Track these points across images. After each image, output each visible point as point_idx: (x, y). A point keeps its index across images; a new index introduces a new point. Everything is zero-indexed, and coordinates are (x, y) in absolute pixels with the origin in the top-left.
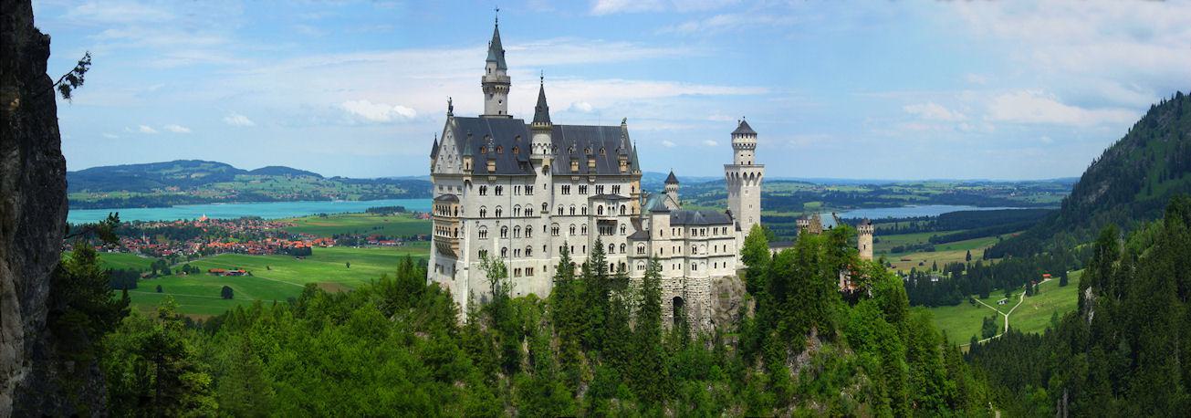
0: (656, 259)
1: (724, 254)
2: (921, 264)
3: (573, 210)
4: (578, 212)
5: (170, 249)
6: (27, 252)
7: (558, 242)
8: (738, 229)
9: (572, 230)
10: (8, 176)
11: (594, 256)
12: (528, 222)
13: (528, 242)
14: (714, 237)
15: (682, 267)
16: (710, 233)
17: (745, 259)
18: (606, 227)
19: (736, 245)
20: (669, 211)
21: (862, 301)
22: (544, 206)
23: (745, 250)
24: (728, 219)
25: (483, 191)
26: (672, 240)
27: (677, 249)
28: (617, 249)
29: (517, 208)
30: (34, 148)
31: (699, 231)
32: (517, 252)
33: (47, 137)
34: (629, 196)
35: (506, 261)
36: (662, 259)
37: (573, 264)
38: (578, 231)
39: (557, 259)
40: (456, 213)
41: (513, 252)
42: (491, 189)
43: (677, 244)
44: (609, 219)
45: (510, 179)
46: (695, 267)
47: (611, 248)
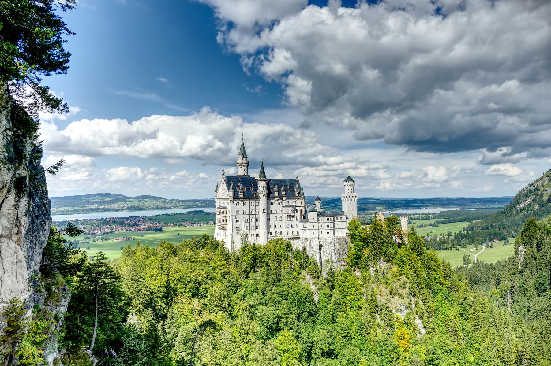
2: (431, 233)
3: (276, 211)
4: (278, 212)
5: (94, 230)
6: (31, 242)
8: (347, 218)
9: (276, 219)
10: (21, 209)
12: (257, 216)
13: (257, 224)
15: (323, 232)
19: (346, 224)
21: (403, 246)
22: (264, 210)
24: (342, 214)
25: (238, 204)
30: (34, 197)
33: (41, 191)
38: (278, 219)
40: (226, 213)
42: (241, 203)
43: (320, 224)
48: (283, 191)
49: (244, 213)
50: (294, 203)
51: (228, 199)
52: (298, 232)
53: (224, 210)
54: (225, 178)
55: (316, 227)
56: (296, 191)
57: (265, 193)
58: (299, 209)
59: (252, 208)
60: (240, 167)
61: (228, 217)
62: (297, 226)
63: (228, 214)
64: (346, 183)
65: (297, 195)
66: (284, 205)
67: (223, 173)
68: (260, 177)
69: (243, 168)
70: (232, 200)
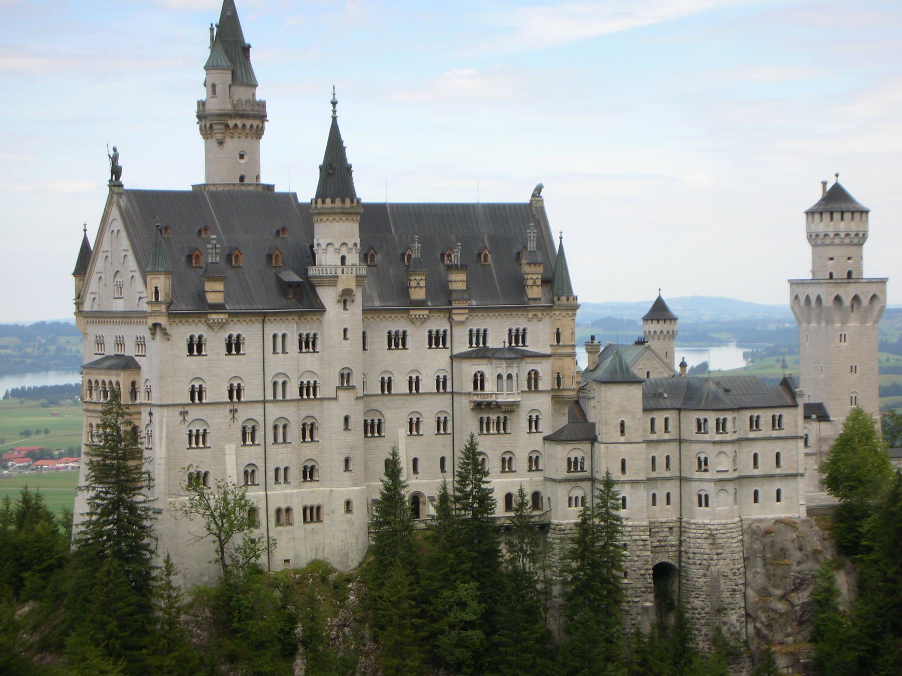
0: (609, 483)
1: (778, 471)
3: (414, 384)
4: (428, 384)
7: (381, 450)
8: (815, 412)
9: (414, 426)
11: (463, 479)
12: (308, 409)
13: (309, 451)
14: (752, 435)
15: (674, 498)
16: (738, 423)
17: (833, 483)
18: (493, 417)
20: (639, 382)
22: (345, 377)
23: (834, 462)
25: (196, 347)
26: (645, 442)
27: (661, 462)
28: (520, 463)
29: (280, 381)
31: (711, 424)
32: (281, 475)
34: (548, 351)
35: (254, 495)
36: (624, 482)
37: (416, 499)
38: (428, 426)
39: (377, 487)
40: (134, 393)
41: (271, 474)
42: (215, 343)
43: (661, 453)
44: (500, 399)
45: (263, 317)
46: (703, 500)
47: (507, 464)
48: (451, 268)
49: (235, 392)
50: (519, 336)
51: (143, 315)
52: (536, 496)
53: (123, 379)
54: (123, 202)
55: (638, 468)
56: (526, 269)
57: (347, 281)
58: (545, 369)
59: (277, 363)
60: (219, 136)
61: (145, 418)
62: (534, 463)
63: (141, 398)
64: (824, 226)
65: (534, 292)
66: (462, 346)
67: (116, 171)
68: (323, 192)
69: (233, 144)
70: (163, 321)
